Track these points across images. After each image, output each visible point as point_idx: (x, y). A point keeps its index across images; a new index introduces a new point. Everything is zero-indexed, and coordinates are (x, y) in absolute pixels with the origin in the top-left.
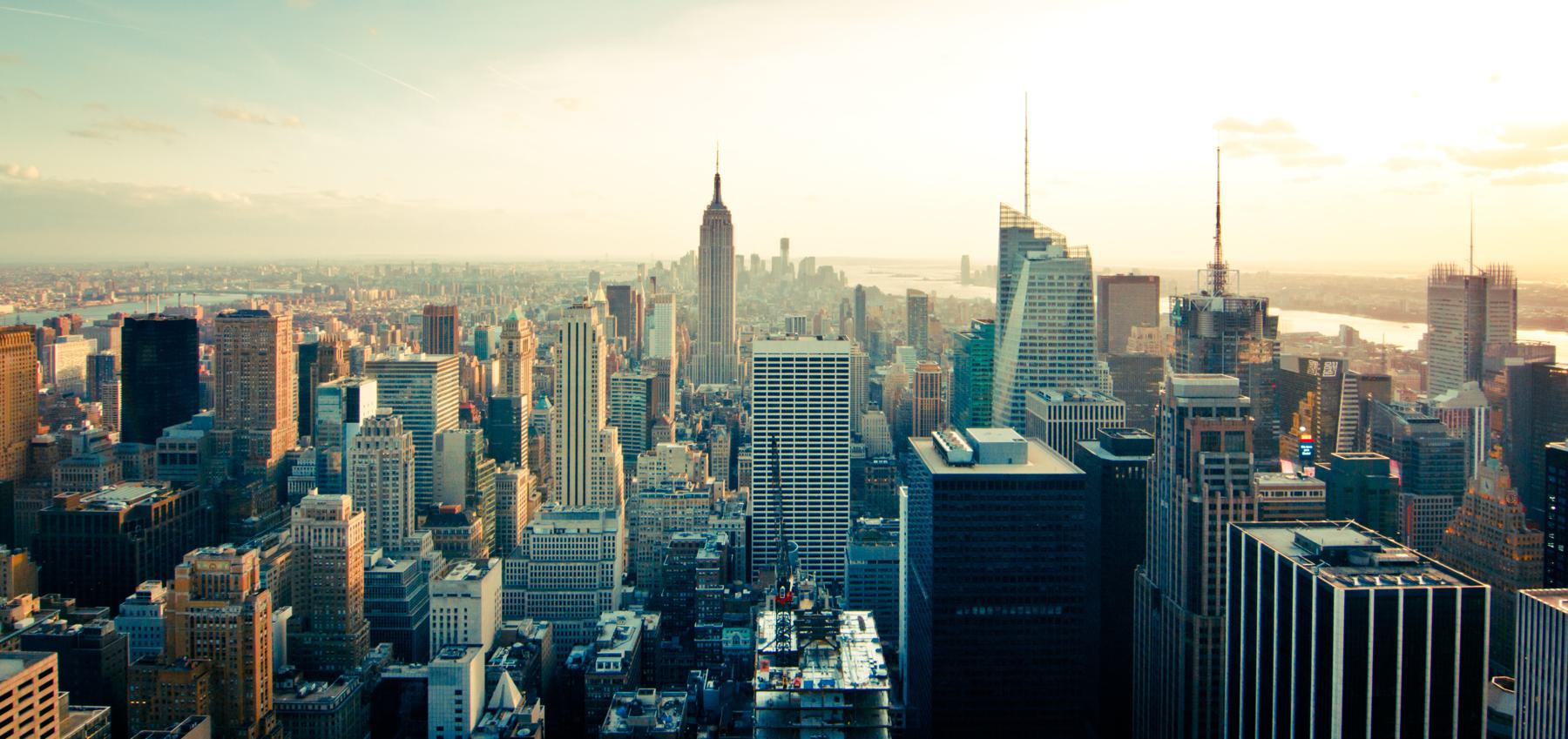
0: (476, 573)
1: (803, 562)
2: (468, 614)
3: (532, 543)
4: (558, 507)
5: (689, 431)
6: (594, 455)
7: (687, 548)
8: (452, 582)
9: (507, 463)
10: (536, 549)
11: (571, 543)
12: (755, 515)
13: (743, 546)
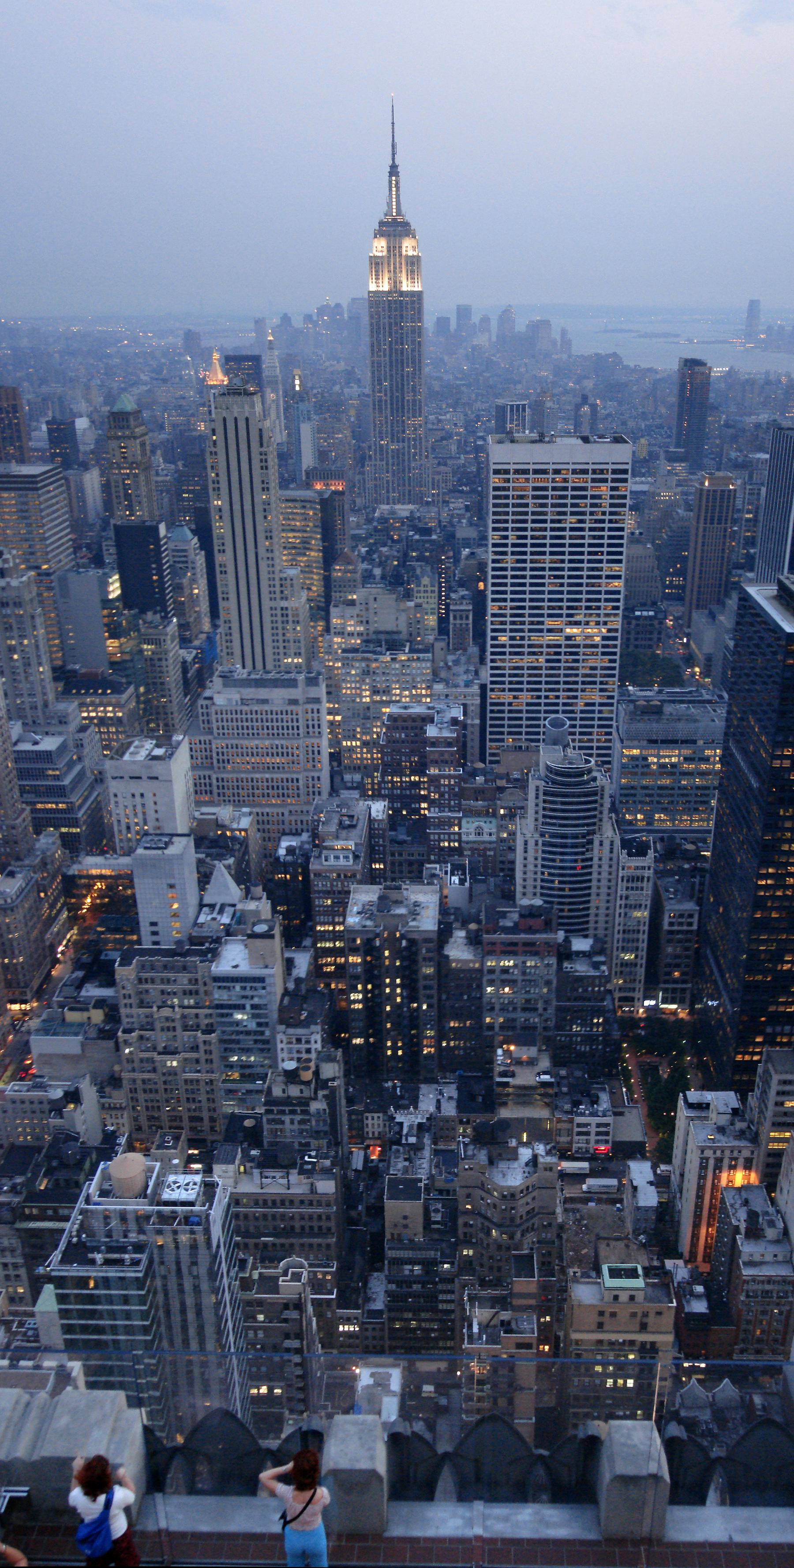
0: (159, 752)
1: (574, 741)
2: (158, 808)
3: (213, 718)
4: (241, 673)
5: (377, 572)
6: (273, 604)
7: (409, 724)
8: (134, 762)
9: (149, 616)
10: (220, 724)
11: (264, 717)
12: (492, 683)
13: (477, 721)
